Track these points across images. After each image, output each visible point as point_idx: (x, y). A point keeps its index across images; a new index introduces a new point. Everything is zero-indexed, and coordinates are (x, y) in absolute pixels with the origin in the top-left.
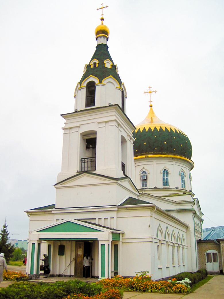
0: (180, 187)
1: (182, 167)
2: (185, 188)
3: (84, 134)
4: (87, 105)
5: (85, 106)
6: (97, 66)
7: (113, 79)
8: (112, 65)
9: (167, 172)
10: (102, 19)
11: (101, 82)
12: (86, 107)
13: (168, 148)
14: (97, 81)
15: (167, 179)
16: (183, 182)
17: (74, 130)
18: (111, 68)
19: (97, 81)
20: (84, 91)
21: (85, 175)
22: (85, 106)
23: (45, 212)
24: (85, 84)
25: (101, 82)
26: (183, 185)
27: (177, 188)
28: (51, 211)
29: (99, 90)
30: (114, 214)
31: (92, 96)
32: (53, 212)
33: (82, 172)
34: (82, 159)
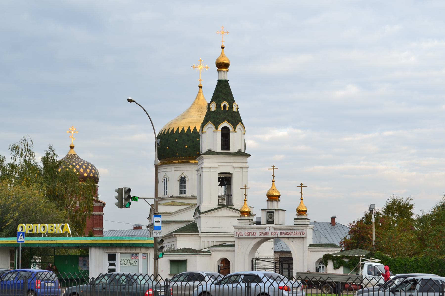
4: (223, 148)
6: (227, 109)
10: (223, 48)
14: (231, 129)
17: (213, 169)
19: (231, 129)
20: (219, 135)
23: (192, 234)
24: (220, 128)
25: (235, 130)
33: (221, 206)
34: (219, 194)
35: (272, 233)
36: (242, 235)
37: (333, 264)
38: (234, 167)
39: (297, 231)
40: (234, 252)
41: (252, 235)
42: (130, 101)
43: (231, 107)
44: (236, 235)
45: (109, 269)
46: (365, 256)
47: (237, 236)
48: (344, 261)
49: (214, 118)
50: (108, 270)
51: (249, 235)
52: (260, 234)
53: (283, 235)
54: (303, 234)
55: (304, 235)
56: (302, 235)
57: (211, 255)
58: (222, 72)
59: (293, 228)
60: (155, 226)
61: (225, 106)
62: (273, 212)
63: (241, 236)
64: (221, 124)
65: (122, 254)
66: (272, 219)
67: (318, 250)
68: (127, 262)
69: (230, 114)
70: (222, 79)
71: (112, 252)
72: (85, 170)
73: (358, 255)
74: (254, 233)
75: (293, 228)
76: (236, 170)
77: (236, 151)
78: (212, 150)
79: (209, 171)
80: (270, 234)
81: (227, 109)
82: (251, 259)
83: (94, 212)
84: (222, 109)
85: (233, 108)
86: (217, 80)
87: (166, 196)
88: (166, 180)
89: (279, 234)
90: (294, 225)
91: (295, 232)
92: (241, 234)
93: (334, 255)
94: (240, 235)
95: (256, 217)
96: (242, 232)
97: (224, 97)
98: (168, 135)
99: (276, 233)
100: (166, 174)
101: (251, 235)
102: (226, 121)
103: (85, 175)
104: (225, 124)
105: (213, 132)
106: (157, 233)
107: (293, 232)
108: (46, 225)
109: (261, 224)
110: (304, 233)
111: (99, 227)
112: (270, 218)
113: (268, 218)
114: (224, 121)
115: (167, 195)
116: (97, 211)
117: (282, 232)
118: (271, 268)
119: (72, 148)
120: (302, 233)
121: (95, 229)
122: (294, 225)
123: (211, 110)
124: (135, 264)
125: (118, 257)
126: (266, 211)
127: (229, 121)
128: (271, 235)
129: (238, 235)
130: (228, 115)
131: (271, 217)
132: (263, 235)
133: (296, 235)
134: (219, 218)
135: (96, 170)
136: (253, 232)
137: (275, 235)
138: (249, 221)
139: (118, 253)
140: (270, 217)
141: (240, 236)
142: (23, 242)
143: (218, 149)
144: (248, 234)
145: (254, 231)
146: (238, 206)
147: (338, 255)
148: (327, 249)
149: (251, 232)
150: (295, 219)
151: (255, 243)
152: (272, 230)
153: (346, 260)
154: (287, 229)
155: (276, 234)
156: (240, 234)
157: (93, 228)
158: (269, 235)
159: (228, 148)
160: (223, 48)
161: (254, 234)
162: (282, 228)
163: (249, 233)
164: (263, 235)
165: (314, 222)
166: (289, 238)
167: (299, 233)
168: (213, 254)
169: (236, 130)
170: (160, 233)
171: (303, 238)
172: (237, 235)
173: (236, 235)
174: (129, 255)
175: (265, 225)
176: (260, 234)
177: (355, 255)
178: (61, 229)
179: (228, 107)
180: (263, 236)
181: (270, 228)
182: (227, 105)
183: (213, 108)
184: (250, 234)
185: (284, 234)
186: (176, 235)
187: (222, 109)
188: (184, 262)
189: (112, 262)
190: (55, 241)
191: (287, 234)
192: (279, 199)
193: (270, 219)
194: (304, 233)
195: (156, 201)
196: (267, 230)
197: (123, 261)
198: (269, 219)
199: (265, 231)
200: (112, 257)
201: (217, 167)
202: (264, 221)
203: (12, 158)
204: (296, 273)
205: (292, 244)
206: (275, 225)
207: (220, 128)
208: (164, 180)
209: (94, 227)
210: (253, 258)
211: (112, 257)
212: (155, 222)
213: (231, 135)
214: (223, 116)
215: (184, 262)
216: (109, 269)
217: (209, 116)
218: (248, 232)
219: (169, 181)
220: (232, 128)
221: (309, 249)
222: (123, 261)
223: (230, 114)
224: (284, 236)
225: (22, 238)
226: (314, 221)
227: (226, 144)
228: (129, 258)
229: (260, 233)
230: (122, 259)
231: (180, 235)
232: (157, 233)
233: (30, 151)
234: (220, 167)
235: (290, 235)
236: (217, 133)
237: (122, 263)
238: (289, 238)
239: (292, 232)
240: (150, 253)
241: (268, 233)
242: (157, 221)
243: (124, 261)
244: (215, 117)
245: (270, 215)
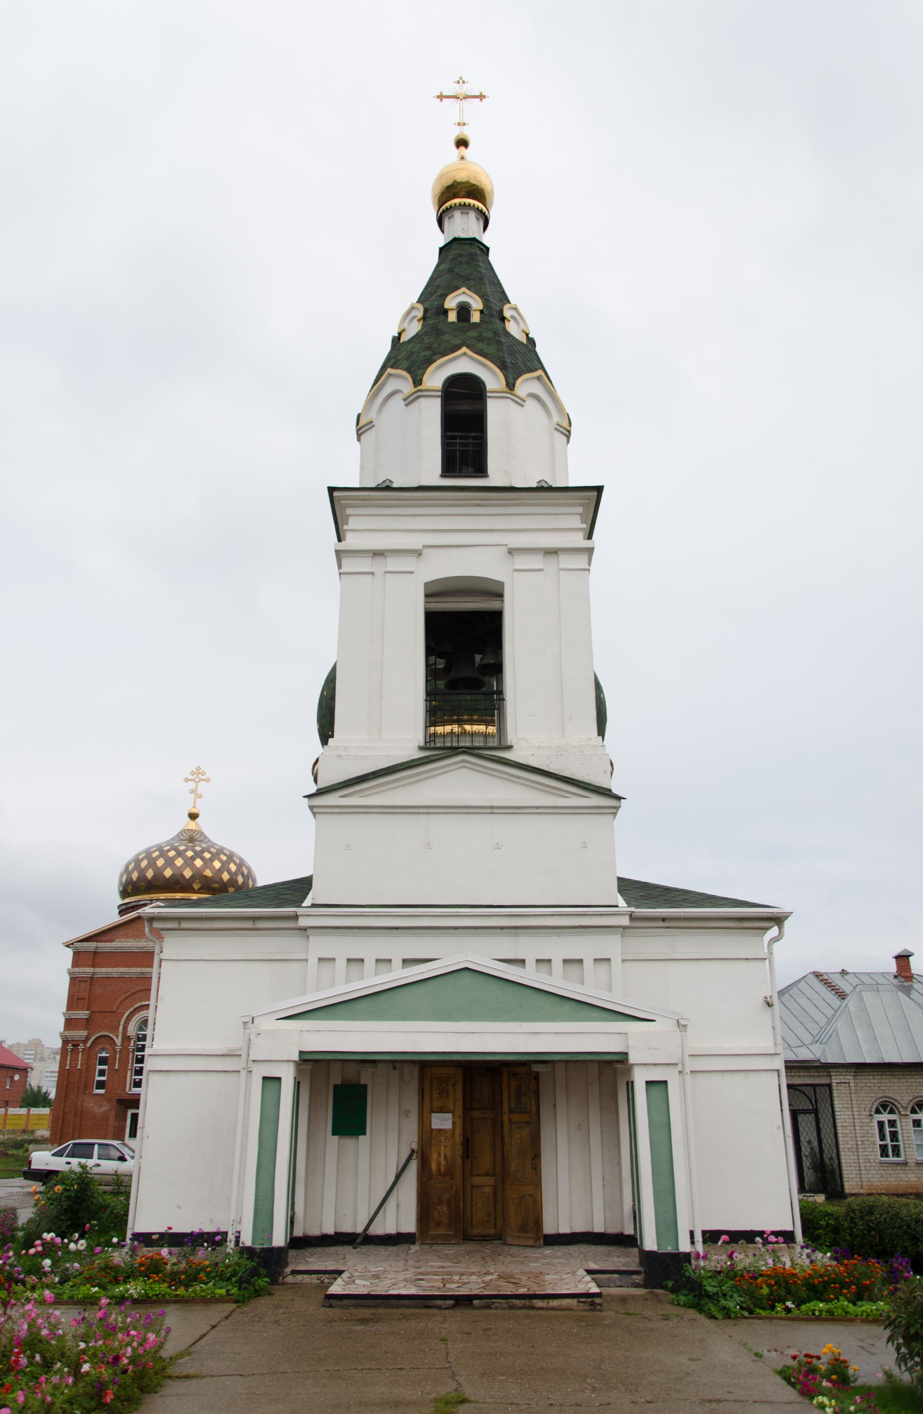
3: (433, 589)
5: (440, 473)
6: (476, 318)
12: (443, 475)
14: (492, 379)
17: (393, 564)
19: (492, 379)
21: (464, 761)
23: (254, 919)
25: (511, 386)
28: (296, 917)
30: (611, 945)
31: (467, 438)
32: (303, 922)
61: (464, 310)
72: (207, 863)
84: (452, 317)
105: (403, 403)
119: (193, 816)
134: (425, 816)
135: (241, 864)
159: (481, 470)
160: (462, 143)
165: (840, 973)
179: (482, 312)
182: (476, 304)
220: (495, 374)
226: (840, 970)
231: (184, 925)
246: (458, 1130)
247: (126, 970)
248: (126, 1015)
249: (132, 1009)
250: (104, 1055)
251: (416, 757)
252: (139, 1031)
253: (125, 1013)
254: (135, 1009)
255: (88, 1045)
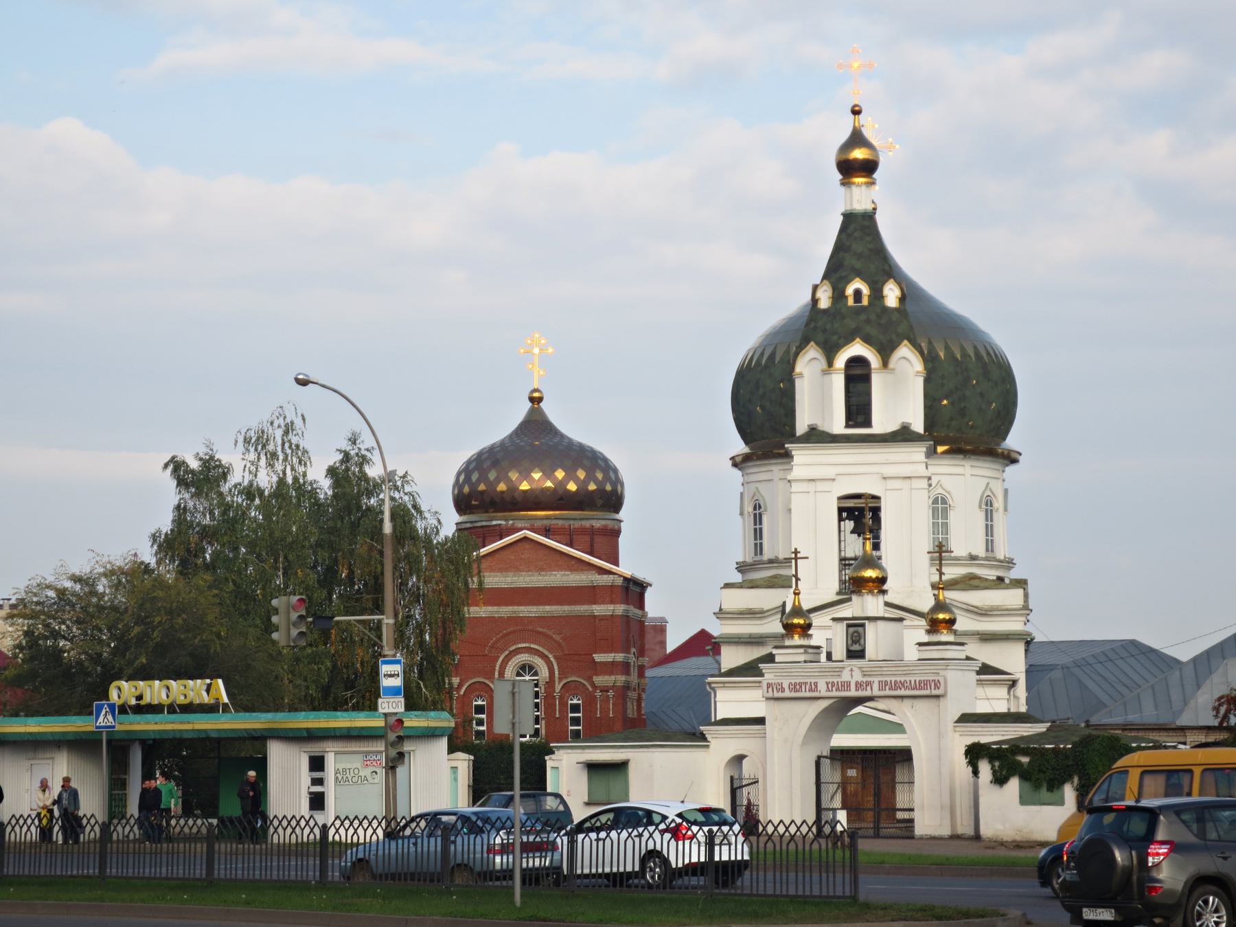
0: (980, 551)
1: (986, 480)
2: (992, 551)
6: (865, 302)
7: (909, 348)
8: (900, 296)
9: (944, 501)
11: (885, 364)
12: (847, 426)
13: (951, 419)
15: (946, 525)
16: (989, 530)
17: (821, 486)
18: (898, 306)
20: (838, 382)
22: (844, 423)
24: (841, 361)
25: (885, 364)
26: (990, 546)
27: (973, 558)
29: (878, 384)
35: (859, 685)
36: (783, 690)
37: (992, 769)
38: (884, 478)
39: (922, 679)
40: (765, 737)
41: (807, 690)
42: (303, 383)
43: (877, 295)
44: (768, 692)
45: (311, 793)
46: (1070, 746)
47: (770, 694)
48: (1020, 761)
49: (825, 331)
50: (308, 796)
51: (800, 690)
52: (828, 687)
53: (885, 689)
54: (937, 687)
55: (938, 688)
56: (935, 689)
57: (707, 746)
58: (854, 188)
59: (911, 668)
60: (384, 685)
61: (858, 293)
62: (863, 625)
63: (780, 695)
64: (843, 349)
65: (337, 756)
66: (860, 645)
67: (980, 729)
68: (352, 774)
69: (873, 317)
70: (855, 210)
71: (316, 748)
73: (1053, 746)
74: (812, 684)
75: (911, 668)
76: (892, 484)
77: (893, 427)
78: (824, 427)
79: (808, 492)
80: (853, 686)
81: (865, 302)
82: (814, 759)
83: (594, 606)
84: (851, 302)
85: (883, 297)
86: (843, 210)
87: (758, 558)
88: (760, 507)
89: (876, 686)
90: (919, 660)
91: (915, 681)
92: (780, 687)
93: (995, 747)
94: (778, 692)
95: (827, 639)
96: (782, 683)
97: (858, 265)
98: (759, 368)
99: (869, 684)
100: (757, 488)
101: (806, 691)
102: (858, 340)
103: (572, 487)
104: (857, 349)
106: (390, 704)
107: (910, 681)
108: (172, 683)
109: (833, 659)
110: (938, 684)
111: (611, 653)
112: (854, 642)
113: (850, 642)
114: (854, 340)
115: (761, 554)
116: (603, 603)
117: (882, 681)
118: (825, 783)
120: (933, 683)
121: (599, 657)
122: (919, 660)
123: (819, 307)
124: (374, 778)
125: (330, 761)
126: (845, 622)
127: (867, 340)
128: (856, 690)
129: (773, 692)
130: (868, 321)
131: (858, 638)
132: (834, 689)
133: (919, 689)
136: (811, 683)
137: (866, 690)
138: (802, 650)
139: (329, 753)
140: (854, 638)
141: (777, 695)
142: (114, 727)
143: (838, 425)
144: (798, 687)
145: (813, 681)
146: (898, 593)
147: (1003, 746)
148: (994, 727)
149: (806, 683)
150: (920, 644)
151: (816, 713)
152: (858, 677)
153: (1025, 760)
154: (896, 673)
155: (869, 688)
156: (778, 687)
157: (594, 655)
158: (850, 690)
159: (867, 423)
161: (813, 687)
162: (885, 669)
163: (800, 684)
164: (834, 689)
166: (902, 697)
167: (924, 684)
168: (714, 743)
169: (892, 363)
170: (400, 703)
171: (937, 697)
172: (770, 690)
173: (768, 692)
174: (360, 757)
175: (843, 661)
176: (828, 687)
177: (1047, 746)
178: (205, 694)
180: (835, 694)
181: (852, 670)
182: (865, 290)
183: (824, 302)
184: (801, 687)
185: (887, 688)
186: (713, 685)
187: (851, 302)
188: (621, 767)
189: (317, 775)
190: (189, 723)
191: (898, 685)
192: (885, 587)
193: (856, 644)
194: (938, 684)
195: (387, 624)
196: (846, 676)
197: (341, 772)
198: (852, 645)
199: (840, 680)
200: (317, 764)
201: (834, 480)
202: (839, 652)
203: (247, 469)
204: (1052, 791)
205: (909, 715)
206: (869, 661)
207: (841, 361)
208: (755, 509)
209: (595, 653)
210: (820, 754)
211: (317, 764)
212: (385, 675)
213: (877, 381)
214: (853, 325)
215: (621, 767)
216: (311, 793)
217: (812, 325)
218: (798, 681)
219: (766, 510)
221: (958, 729)
222: (341, 772)
223: (873, 317)
224: (888, 692)
225: (110, 717)
227: (858, 411)
228: (359, 765)
229: (827, 683)
230: (340, 767)
231: (726, 685)
232: (390, 704)
233: (298, 446)
234: (838, 476)
235: (903, 689)
236: (833, 375)
237: (340, 778)
238: (902, 697)
239: (908, 682)
240: (417, 752)
241: (849, 684)
242: (389, 673)
243: (344, 773)
244: (828, 326)
245: (855, 634)
246: (860, 776)
247: (495, 608)
248: (501, 659)
249: (507, 652)
250: (480, 703)
251: (835, 599)
252: (516, 676)
253: (499, 657)
254: (510, 652)
255: (462, 693)
